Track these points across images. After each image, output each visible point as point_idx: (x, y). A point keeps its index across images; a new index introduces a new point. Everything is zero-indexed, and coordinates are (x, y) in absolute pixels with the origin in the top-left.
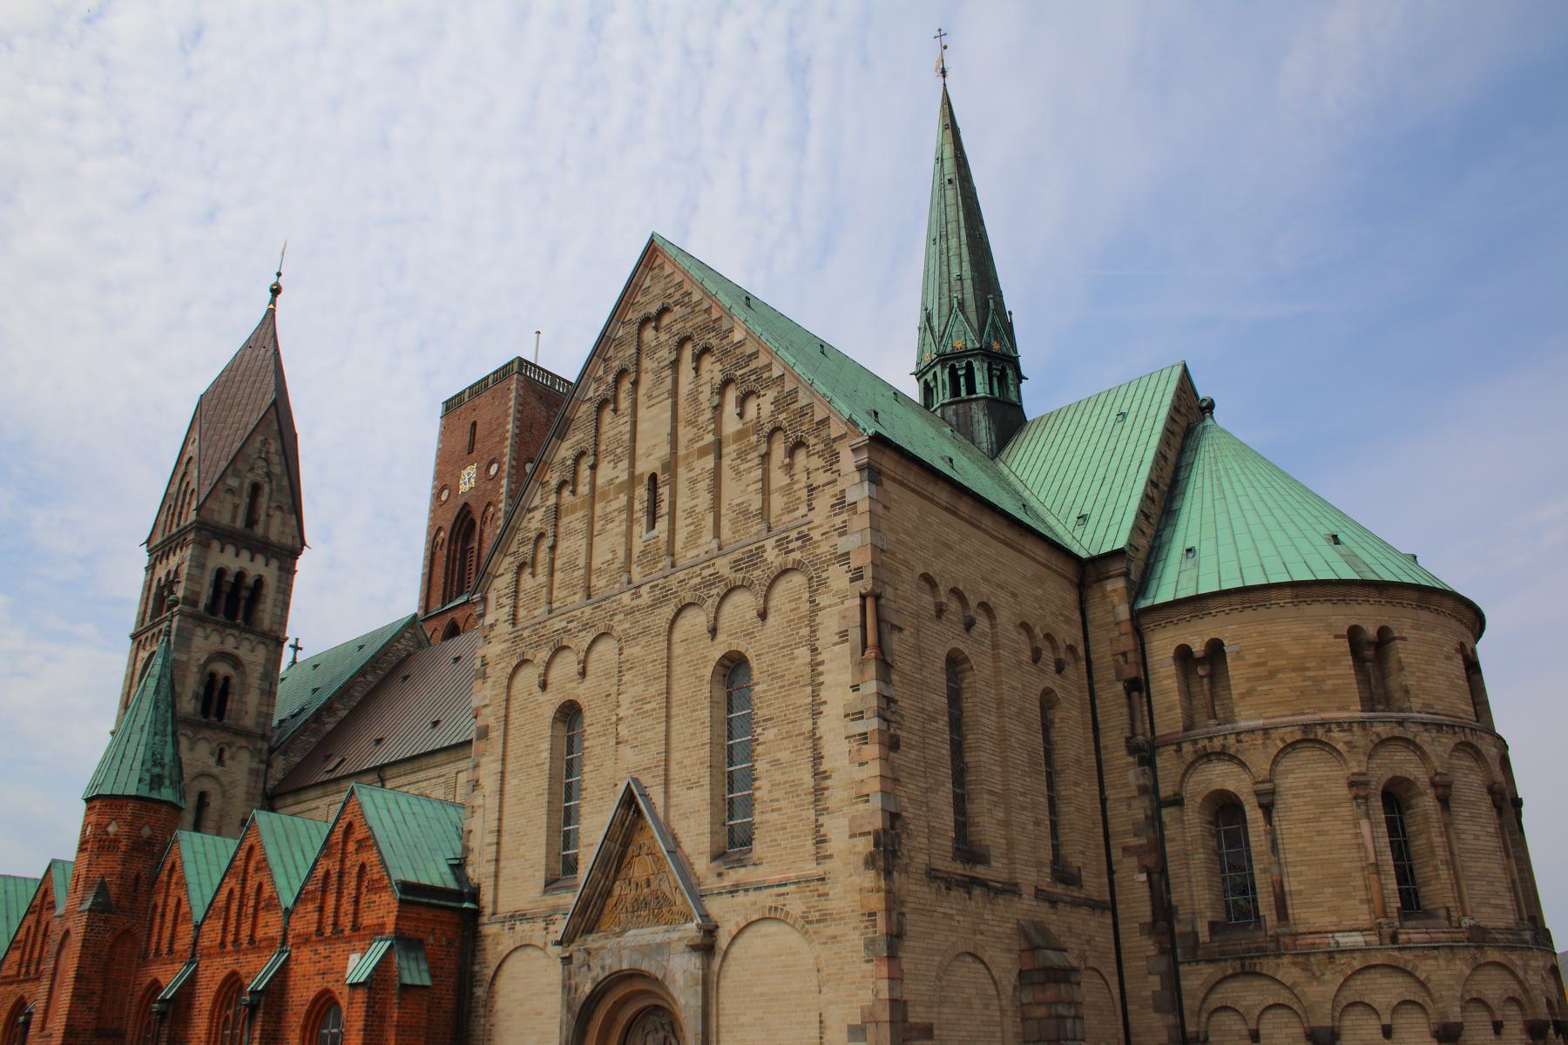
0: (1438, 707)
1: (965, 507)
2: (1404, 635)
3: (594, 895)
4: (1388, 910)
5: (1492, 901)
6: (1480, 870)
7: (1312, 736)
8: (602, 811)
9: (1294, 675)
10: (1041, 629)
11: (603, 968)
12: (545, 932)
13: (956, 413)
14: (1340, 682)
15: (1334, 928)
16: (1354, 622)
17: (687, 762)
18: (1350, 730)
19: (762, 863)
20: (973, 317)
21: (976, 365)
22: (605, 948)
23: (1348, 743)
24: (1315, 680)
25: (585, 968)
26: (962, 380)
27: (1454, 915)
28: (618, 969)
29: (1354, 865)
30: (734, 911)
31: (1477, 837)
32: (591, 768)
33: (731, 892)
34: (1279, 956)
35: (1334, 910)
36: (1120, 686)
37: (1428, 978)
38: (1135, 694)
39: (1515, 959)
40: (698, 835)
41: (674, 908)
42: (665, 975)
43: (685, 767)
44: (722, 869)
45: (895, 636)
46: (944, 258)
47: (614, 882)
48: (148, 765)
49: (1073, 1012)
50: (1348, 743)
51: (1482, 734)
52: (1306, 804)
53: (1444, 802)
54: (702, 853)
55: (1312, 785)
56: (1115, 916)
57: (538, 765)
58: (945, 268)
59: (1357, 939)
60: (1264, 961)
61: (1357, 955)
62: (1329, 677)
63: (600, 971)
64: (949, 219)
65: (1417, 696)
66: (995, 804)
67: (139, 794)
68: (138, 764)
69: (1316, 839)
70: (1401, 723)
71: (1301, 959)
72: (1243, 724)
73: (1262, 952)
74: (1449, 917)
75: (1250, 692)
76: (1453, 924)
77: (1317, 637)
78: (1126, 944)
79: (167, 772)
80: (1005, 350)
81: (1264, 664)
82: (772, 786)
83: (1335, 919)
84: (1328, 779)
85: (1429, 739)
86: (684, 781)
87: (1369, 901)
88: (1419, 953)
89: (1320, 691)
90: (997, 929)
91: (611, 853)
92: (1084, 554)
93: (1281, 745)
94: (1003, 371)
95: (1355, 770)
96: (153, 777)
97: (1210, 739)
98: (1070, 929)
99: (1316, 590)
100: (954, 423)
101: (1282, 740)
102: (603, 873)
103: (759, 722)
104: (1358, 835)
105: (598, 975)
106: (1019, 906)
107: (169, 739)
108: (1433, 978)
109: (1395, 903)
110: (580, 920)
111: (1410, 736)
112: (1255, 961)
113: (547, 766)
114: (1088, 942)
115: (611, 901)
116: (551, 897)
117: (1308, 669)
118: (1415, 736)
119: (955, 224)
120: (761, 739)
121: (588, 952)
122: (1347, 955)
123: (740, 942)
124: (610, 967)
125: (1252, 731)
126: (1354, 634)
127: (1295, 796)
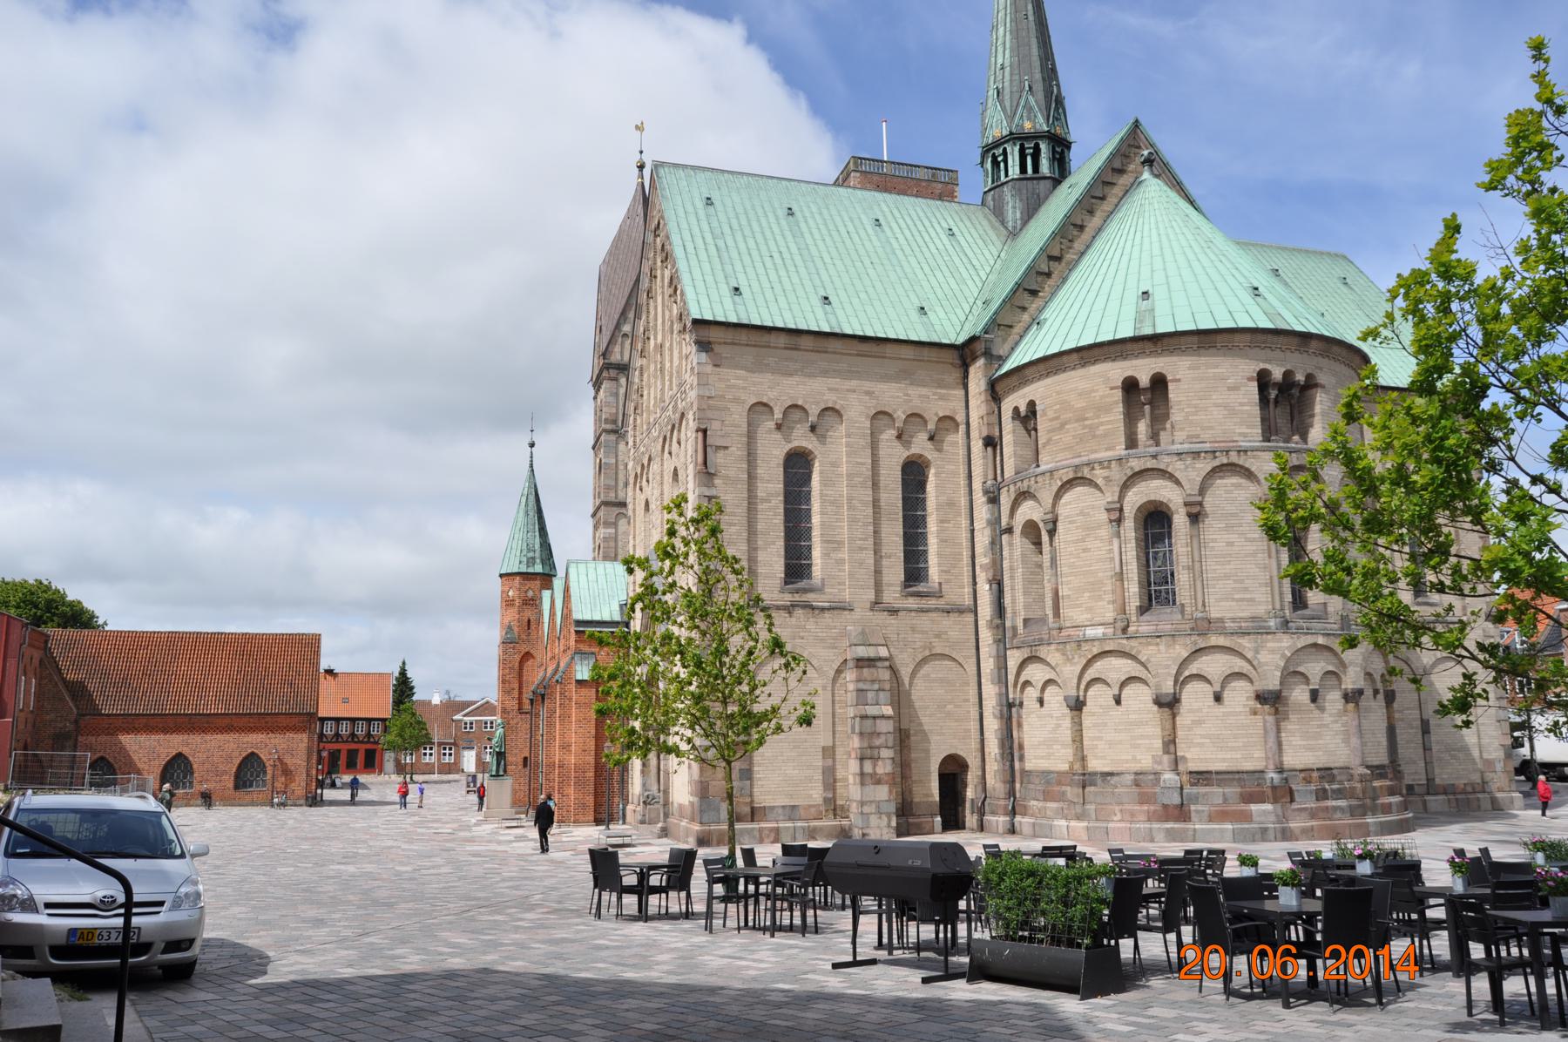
0: (1205, 436)
1: (806, 342)
2: (1178, 377)
4: (1127, 608)
5: (1236, 596)
6: (1228, 571)
7: (1079, 475)
9: (1076, 425)
10: (904, 413)
13: (994, 200)
14: (1110, 426)
15: (1089, 623)
16: (1129, 373)
18: (1109, 467)
20: (1007, 104)
21: (1009, 150)
23: (1104, 478)
24: (1091, 427)
26: (1002, 165)
27: (1188, 609)
29: (1106, 574)
31: (1230, 544)
34: (1049, 644)
35: (1089, 609)
36: (980, 443)
37: (1148, 659)
38: (989, 449)
39: (1246, 644)
45: (721, 454)
46: (994, 48)
48: (525, 552)
49: (876, 686)
50: (1104, 478)
51: (1255, 453)
52: (1077, 528)
53: (1195, 518)
55: (1082, 513)
56: (976, 615)
58: (993, 59)
59: (1099, 632)
60: (1041, 648)
61: (1096, 643)
62: (1102, 424)
64: (1001, 8)
65: (1182, 429)
66: (835, 550)
67: (521, 571)
68: (518, 554)
69: (1082, 555)
70: (1154, 457)
71: (1061, 647)
72: (1043, 468)
73: (1041, 643)
74: (1182, 612)
75: (1049, 441)
76: (1186, 617)
77: (1097, 390)
78: (981, 636)
79: (537, 554)
80: (1038, 126)
81: (1057, 418)
83: (1089, 616)
84: (1093, 507)
85: (1183, 467)
87: (1114, 602)
88: (1144, 640)
89: (1094, 437)
90: (820, 634)
92: (961, 340)
93: (1060, 484)
94: (1037, 150)
95: (1109, 500)
96: (528, 559)
97: (1022, 480)
98: (913, 629)
99: (1096, 351)
100: (992, 208)
101: (1061, 479)
104: (1111, 551)
106: (848, 617)
107: (537, 534)
108: (1152, 659)
109: (1134, 603)
111: (1162, 466)
112: (1038, 648)
114: (938, 636)
117: (1086, 419)
118: (1167, 466)
119: (1003, 12)
122: (1090, 643)
125: (1044, 474)
126: (1130, 386)
127: (1070, 522)
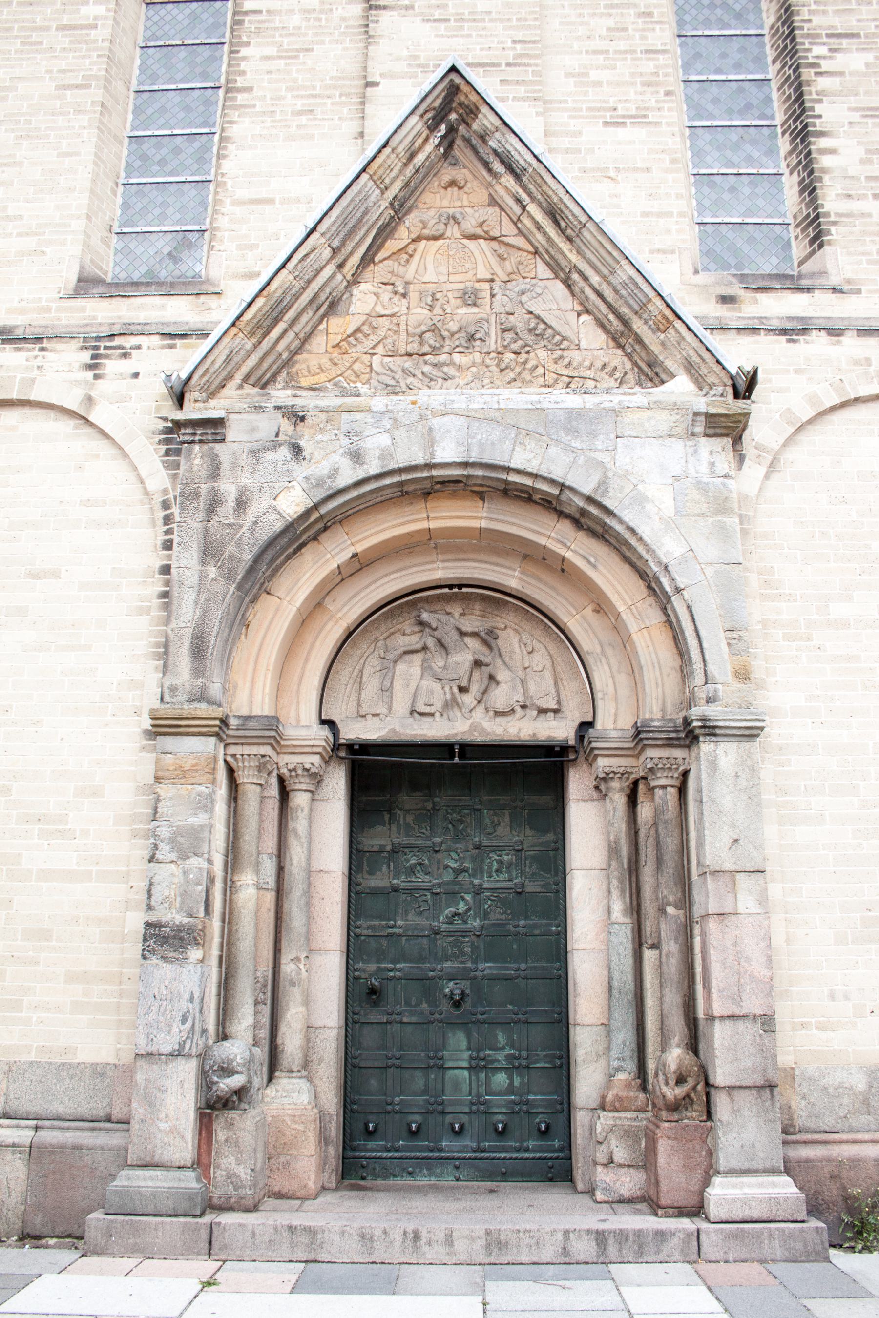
3: (297, 297)
8: (312, 137)
11: (356, 456)
12: (90, 374)
17: (594, 75)
19: (859, 291)
22: (369, 411)
25: (284, 452)
28: (420, 459)
30: (797, 371)
32: (272, 51)
33: (784, 331)
40: (645, 214)
41: (575, 356)
42: (603, 484)
43: (598, 84)
44: (735, 289)
47: (355, 281)
54: (659, 251)
57: (62, 28)
63: (345, 464)
82: (868, 151)
86: (590, 109)
91: (366, 213)
102: (335, 252)
103: (818, 36)
105: (334, 473)
110: (249, 345)
113: (102, 33)
115: (337, 326)
116: (105, 304)
120: (825, 65)
121: (297, 417)
123: (815, 436)
124: (384, 455)
